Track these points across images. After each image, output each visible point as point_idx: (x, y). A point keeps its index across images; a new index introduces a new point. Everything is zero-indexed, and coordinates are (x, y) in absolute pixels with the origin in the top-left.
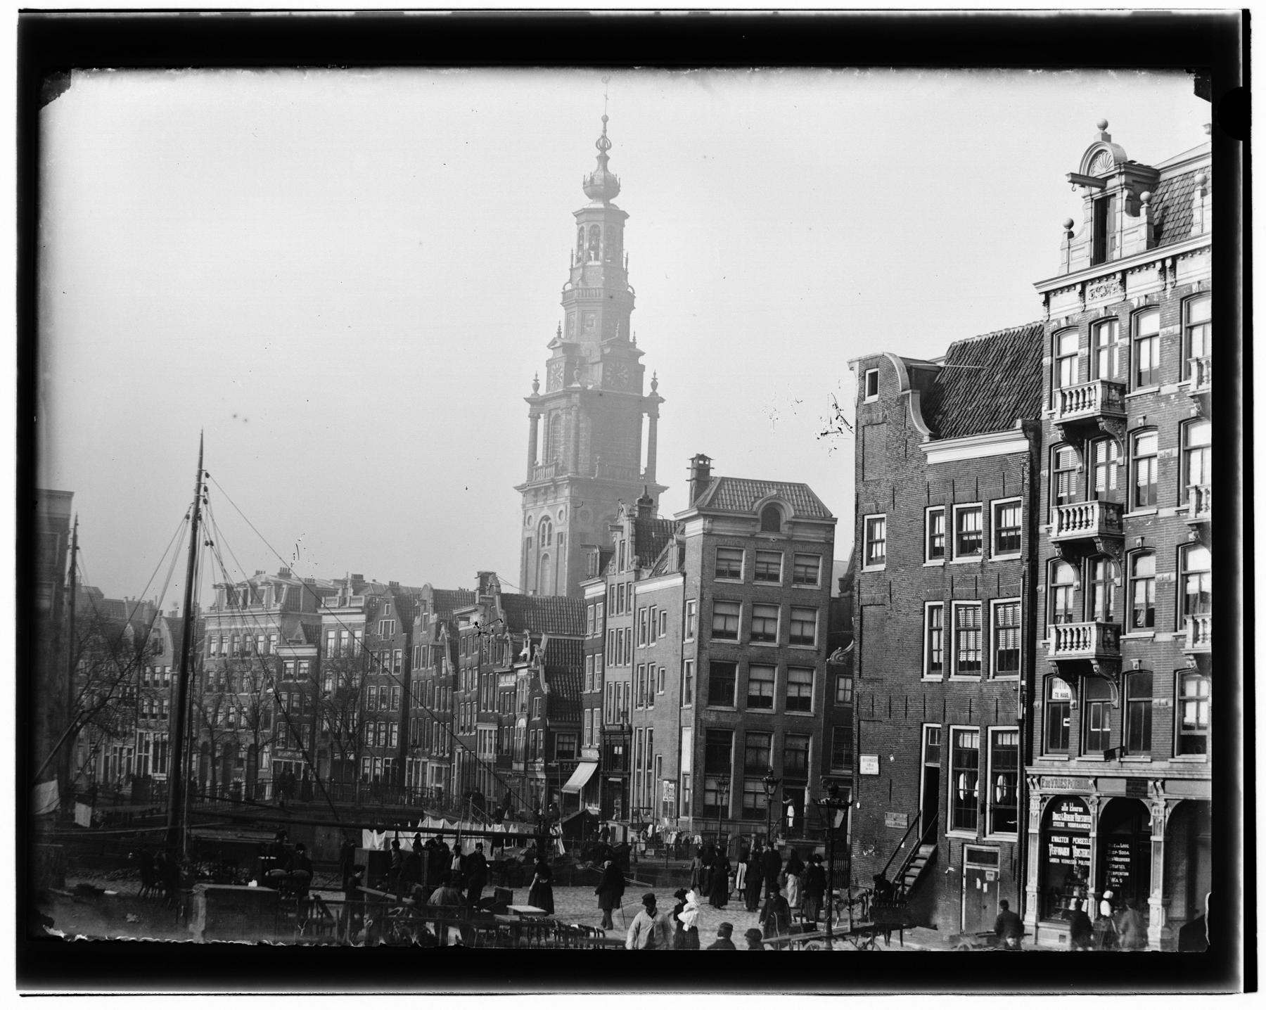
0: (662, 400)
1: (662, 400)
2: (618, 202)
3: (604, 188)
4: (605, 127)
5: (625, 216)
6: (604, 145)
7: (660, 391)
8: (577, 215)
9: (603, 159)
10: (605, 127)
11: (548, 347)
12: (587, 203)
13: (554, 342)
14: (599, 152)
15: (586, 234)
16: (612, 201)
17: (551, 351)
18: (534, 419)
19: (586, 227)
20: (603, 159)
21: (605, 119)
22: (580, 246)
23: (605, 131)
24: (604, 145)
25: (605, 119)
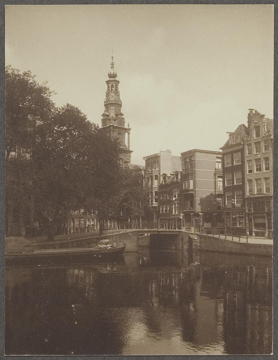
0: (130, 129)
1: (130, 129)
3: (113, 76)
5: (118, 82)
6: (112, 64)
10: (112, 59)
11: (102, 116)
12: (108, 79)
13: (104, 114)
15: (110, 87)
16: (116, 79)
17: (103, 117)
19: (110, 85)
20: (113, 67)
21: (112, 57)
22: (109, 90)
24: (112, 64)
25: (112, 57)
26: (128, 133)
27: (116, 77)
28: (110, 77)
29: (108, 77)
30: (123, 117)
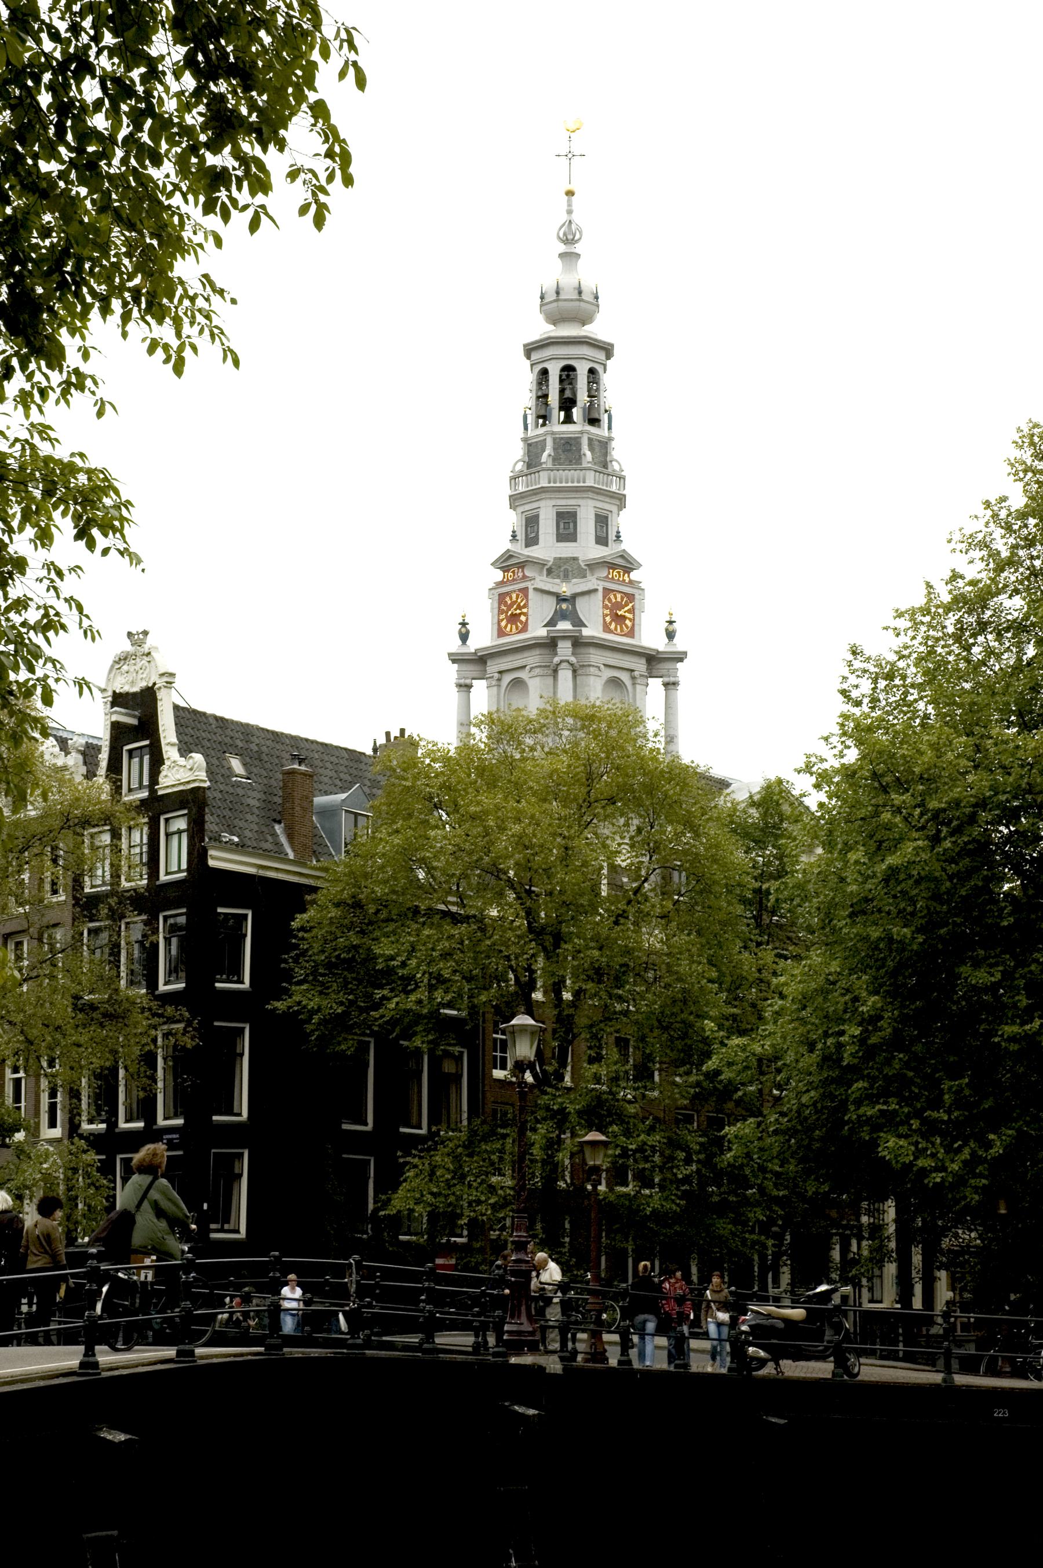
2: (596, 330)
4: (569, 205)
5: (608, 350)
6: (569, 238)
7: (680, 644)
8: (529, 350)
9: (569, 257)
10: (569, 205)
12: (541, 329)
14: (562, 248)
16: (586, 327)
18: (465, 688)
20: (569, 257)
21: (570, 193)
23: (570, 212)
24: (569, 238)
25: (570, 193)
26: (666, 685)
27: (584, 320)
28: (555, 319)
29: (541, 318)
30: (634, 575)
